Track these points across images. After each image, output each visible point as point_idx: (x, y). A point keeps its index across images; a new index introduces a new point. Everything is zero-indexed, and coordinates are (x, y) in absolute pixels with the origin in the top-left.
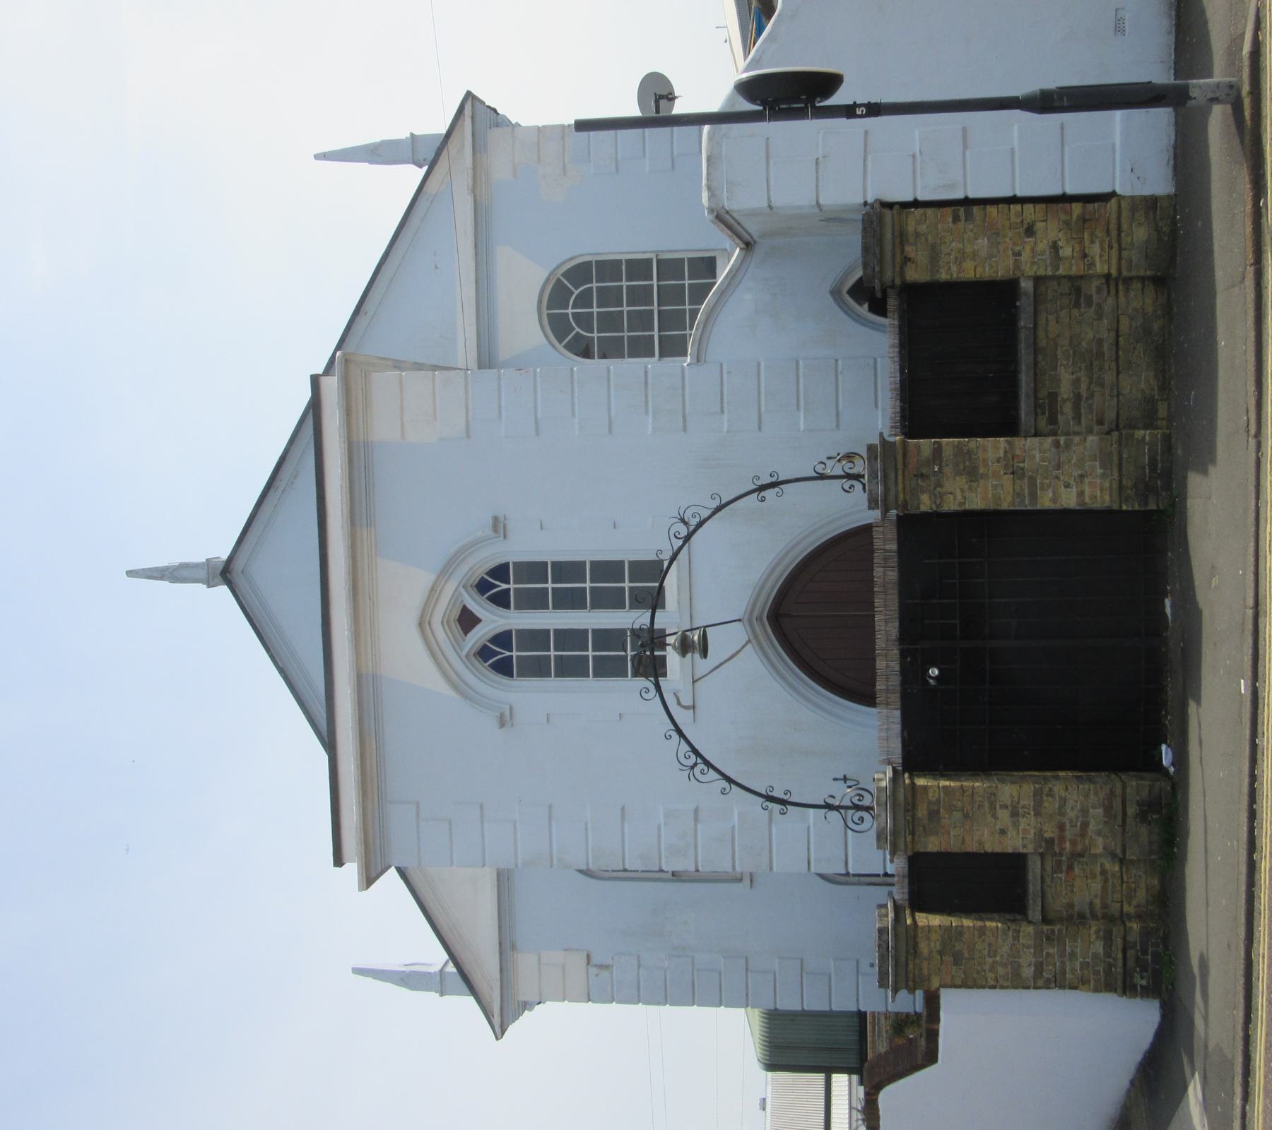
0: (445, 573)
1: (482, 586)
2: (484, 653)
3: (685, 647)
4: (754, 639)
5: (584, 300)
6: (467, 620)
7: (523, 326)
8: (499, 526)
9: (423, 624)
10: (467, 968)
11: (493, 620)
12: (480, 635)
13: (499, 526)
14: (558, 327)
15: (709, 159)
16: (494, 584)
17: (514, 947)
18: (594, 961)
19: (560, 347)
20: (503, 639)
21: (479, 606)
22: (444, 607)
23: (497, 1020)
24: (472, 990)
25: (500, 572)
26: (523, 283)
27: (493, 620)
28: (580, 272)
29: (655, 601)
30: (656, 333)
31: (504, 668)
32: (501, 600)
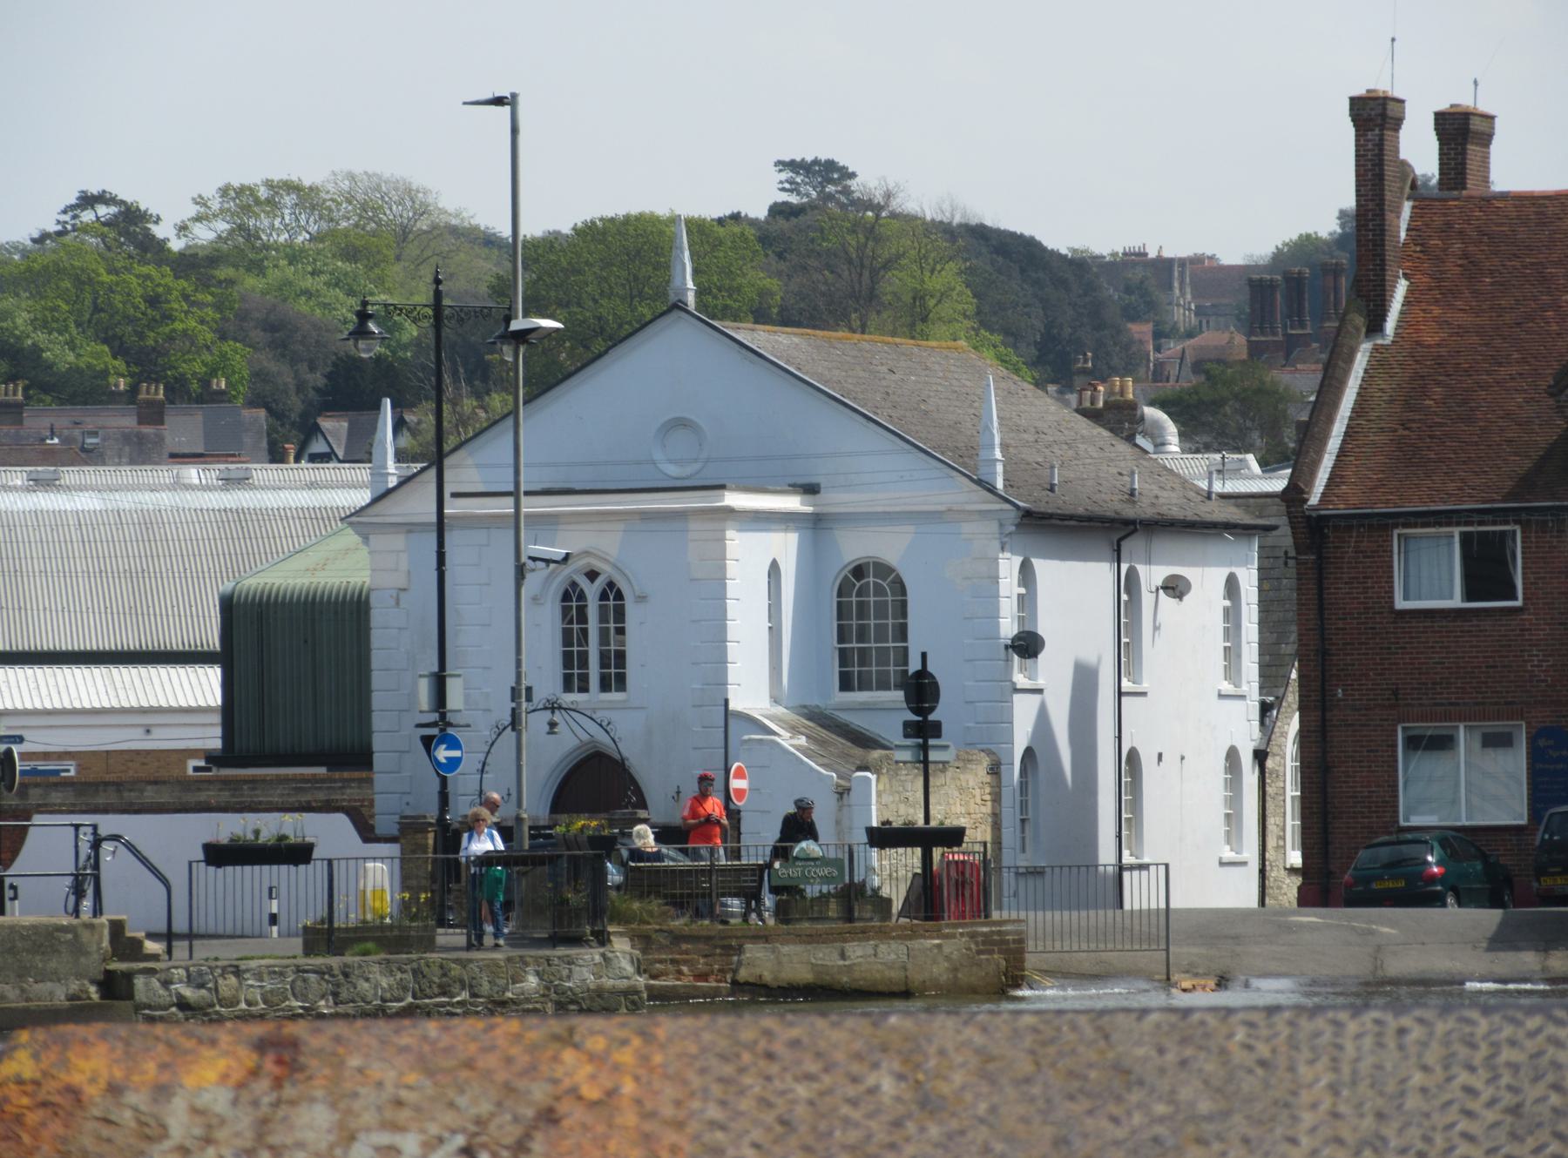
0: (615, 566)
1: (611, 585)
2: (574, 584)
3: (553, 725)
4: (583, 744)
5: (879, 590)
6: (592, 575)
7: (855, 546)
8: (641, 599)
9: (587, 553)
10: (393, 496)
11: (592, 591)
12: (584, 583)
13: (641, 599)
14: (859, 571)
15: (761, 740)
16: (612, 593)
17: (409, 531)
18: (402, 595)
19: (846, 572)
20: (582, 596)
21: (600, 582)
22: (598, 565)
23: (354, 519)
24: (376, 500)
25: (619, 596)
26: (888, 546)
27: (592, 591)
28: (900, 587)
29: (605, 686)
30: (855, 645)
31: (566, 597)
32: (604, 596)
